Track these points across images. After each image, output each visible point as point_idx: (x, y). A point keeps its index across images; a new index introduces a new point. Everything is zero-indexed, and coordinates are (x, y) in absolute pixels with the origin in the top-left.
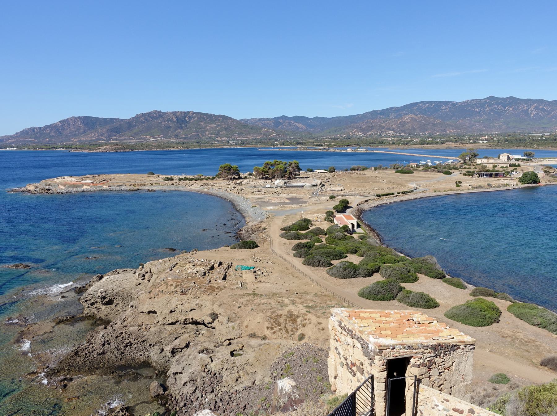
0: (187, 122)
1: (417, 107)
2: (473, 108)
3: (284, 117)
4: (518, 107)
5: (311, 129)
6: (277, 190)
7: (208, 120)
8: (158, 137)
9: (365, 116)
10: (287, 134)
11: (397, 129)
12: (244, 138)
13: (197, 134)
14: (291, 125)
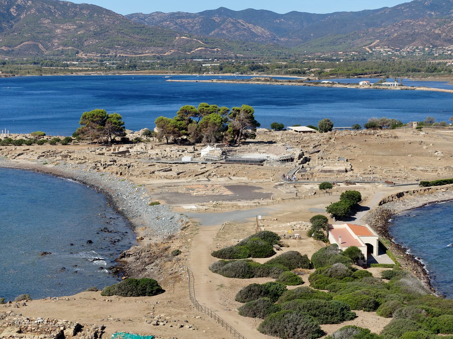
0: (13, 18)
3: (223, 12)
6: (206, 169)
7: (60, 15)
10: (231, 49)
14: (238, 29)
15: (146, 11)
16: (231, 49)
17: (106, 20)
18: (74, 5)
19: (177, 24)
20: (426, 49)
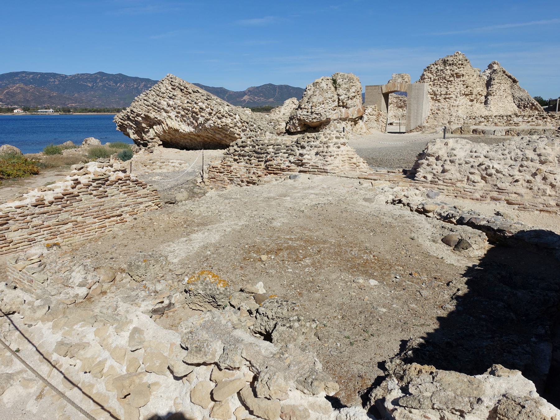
2: (86, 83)
4: (129, 84)
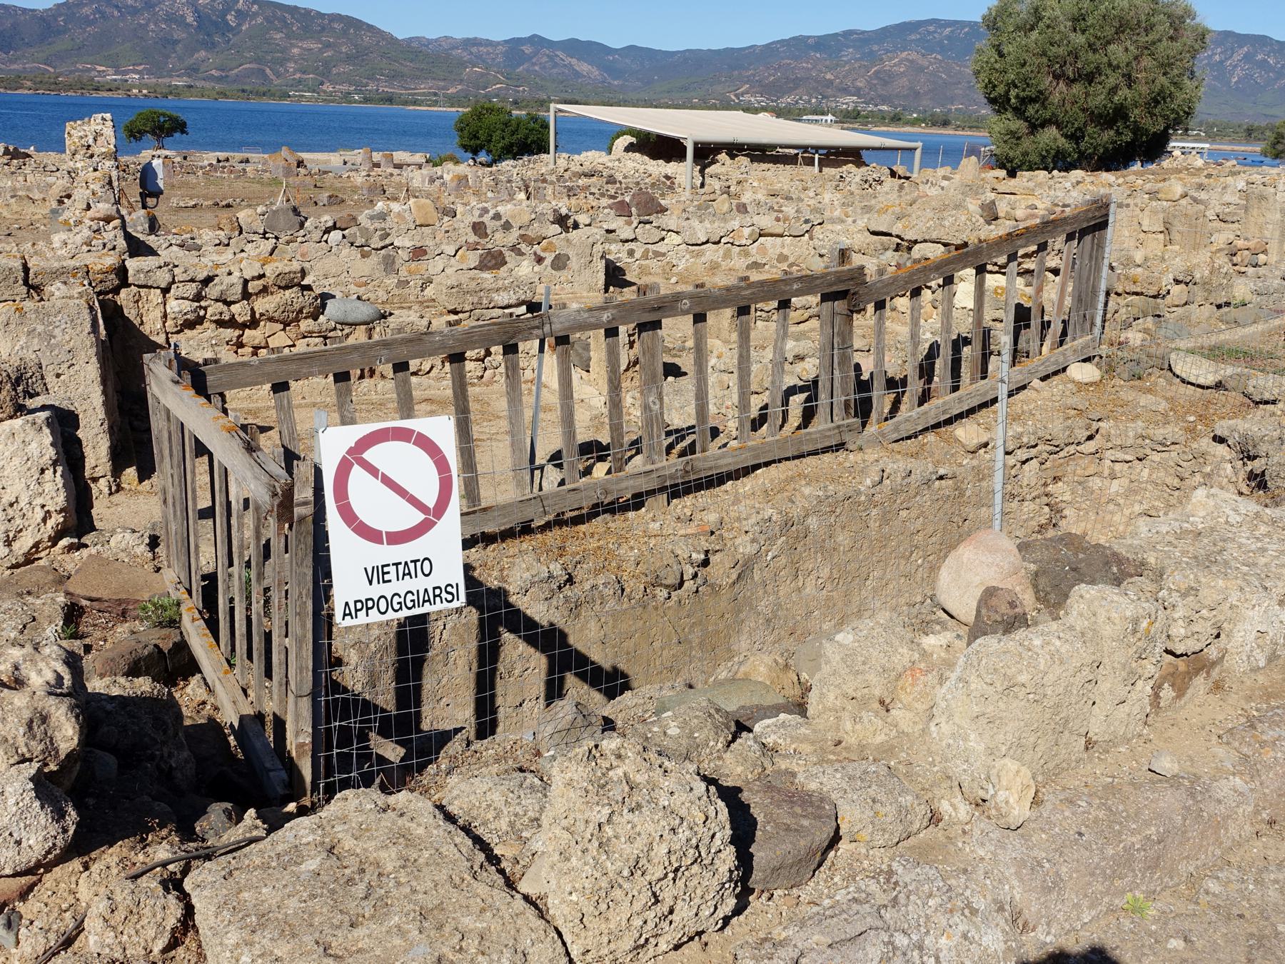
0: (230, 29)
1: (919, 34)
3: (536, 41)
5: (614, 80)
8: (135, 72)
9: (770, 50)
10: (542, 88)
11: (867, 90)
12: (406, 89)
13: (259, 69)
14: (556, 65)
15: (432, 34)
16: (542, 88)
17: (367, 39)
18: (322, 16)
19: (472, 53)
20: (814, 100)
